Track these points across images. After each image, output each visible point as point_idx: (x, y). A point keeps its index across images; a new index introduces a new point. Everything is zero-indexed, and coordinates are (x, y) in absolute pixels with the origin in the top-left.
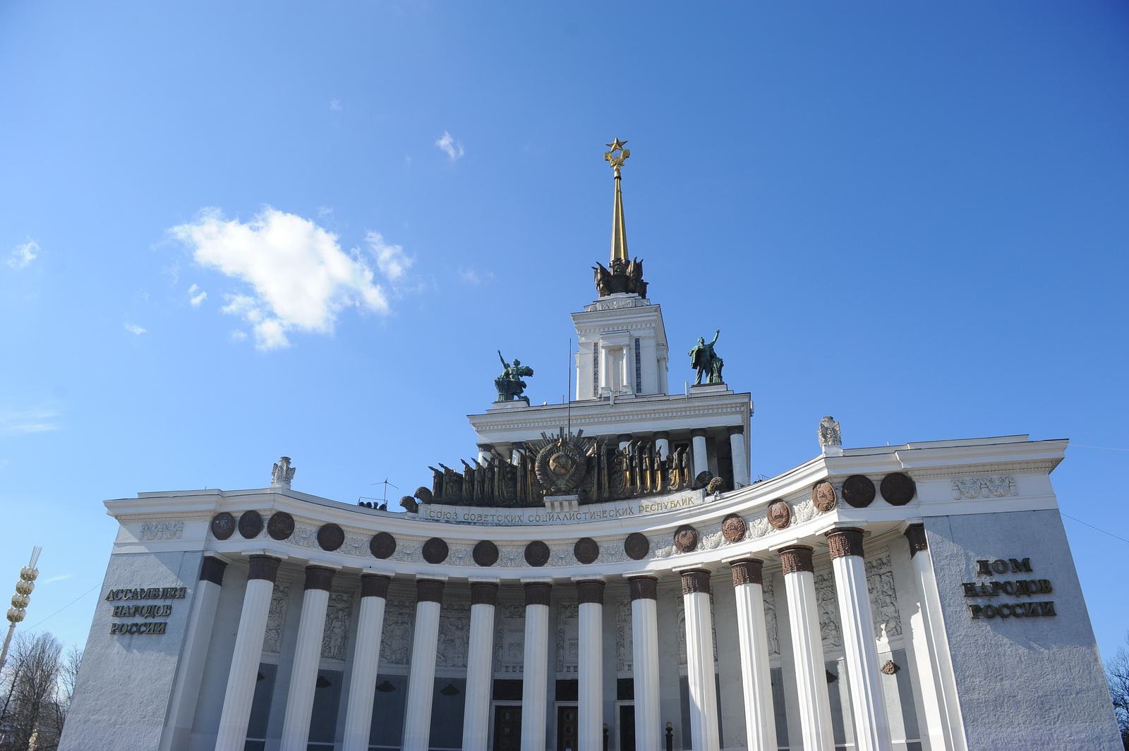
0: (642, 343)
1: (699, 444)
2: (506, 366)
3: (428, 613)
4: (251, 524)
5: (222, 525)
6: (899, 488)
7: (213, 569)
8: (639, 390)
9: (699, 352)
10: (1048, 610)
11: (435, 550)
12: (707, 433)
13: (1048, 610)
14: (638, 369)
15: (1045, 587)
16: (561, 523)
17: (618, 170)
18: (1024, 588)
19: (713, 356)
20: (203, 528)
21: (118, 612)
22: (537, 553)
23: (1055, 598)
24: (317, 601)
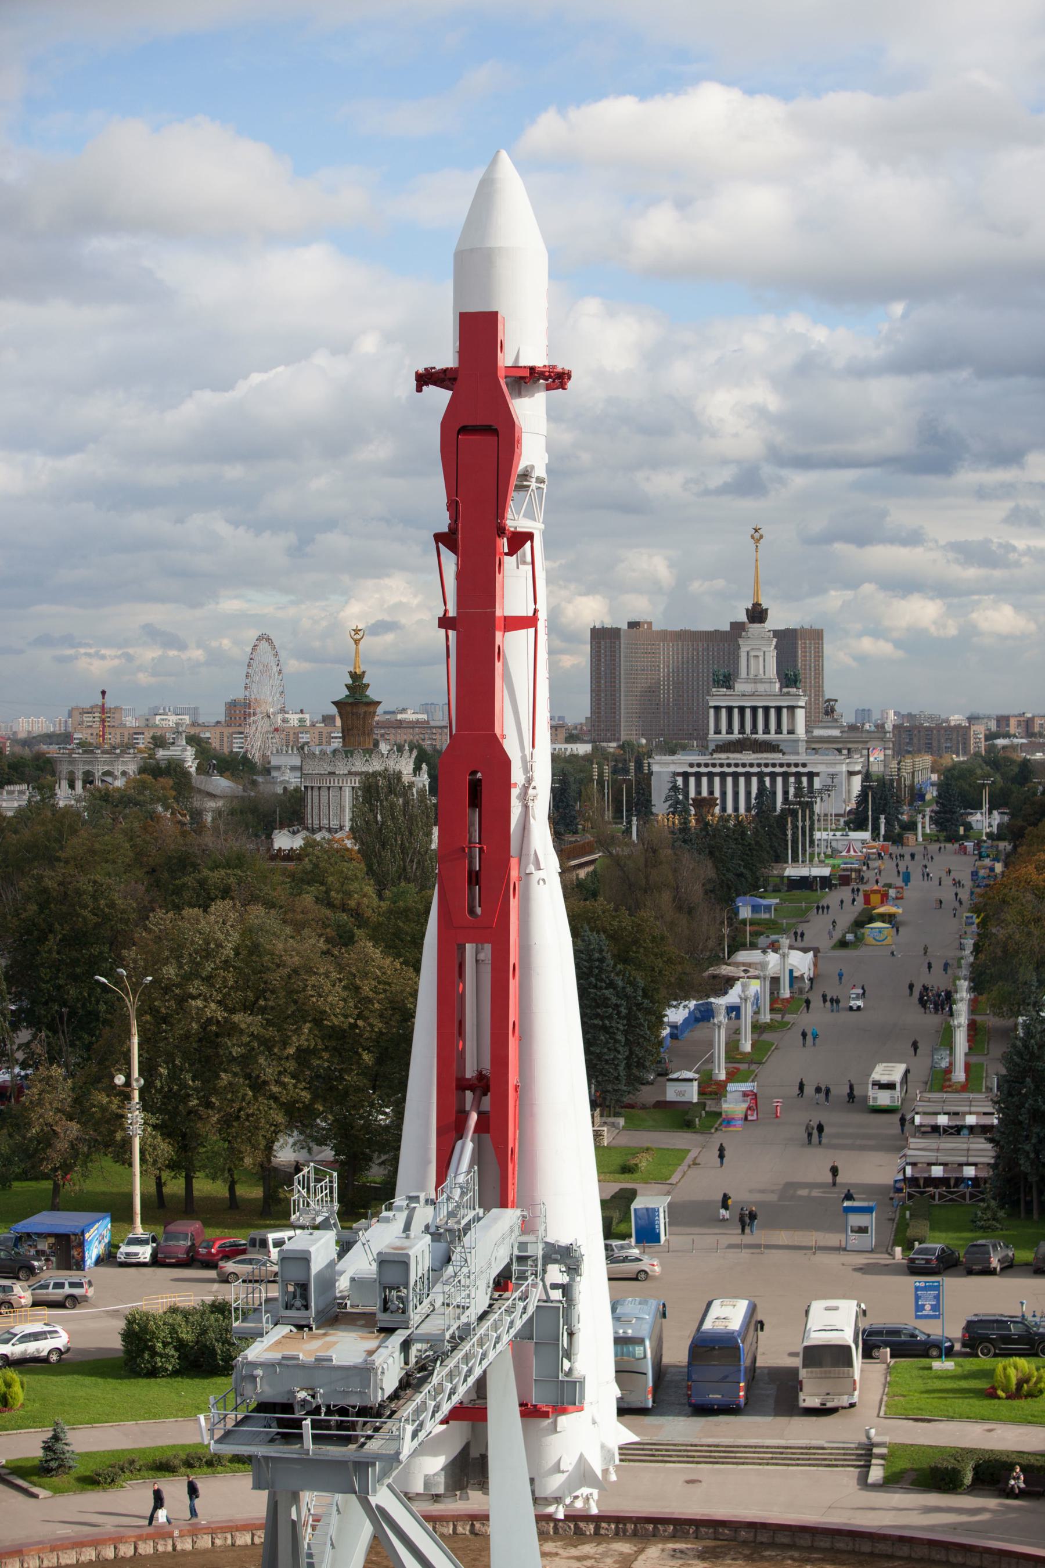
1: (785, 711)
12: (788, 707)
16: (748, 757)
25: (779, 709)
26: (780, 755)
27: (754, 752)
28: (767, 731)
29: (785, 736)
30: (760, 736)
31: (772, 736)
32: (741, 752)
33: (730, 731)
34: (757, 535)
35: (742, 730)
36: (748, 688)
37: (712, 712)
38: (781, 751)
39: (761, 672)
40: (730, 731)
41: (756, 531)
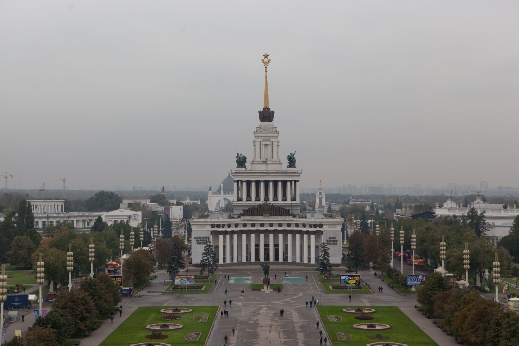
0: (274, 143)
2: (238, 154)
3: (244, 236)
4: (218, 226)
5: (213, 226)
6: (321, 226)
7: (212, 233)
8: (272, 158)
9: (290, 158)
10: (336, 244)
11: (245, 225)
12: (291, 181)
13: (336, 244)
14: (272, 151)
15: (337, 241)
16: (267, 219)
17: (266, 68)
18: (334, 241)
19: (294, 158)
20: (210, 227)
21: (197, 241)
22: (262, 225)
23: (338, 242)
24: (228, 236)
25: (284, 183)
26: (291, 218)
27: (271, 215)
28: (276, 198)
29: (289, 202)
30: (271, 202)
31: (280, 202)
32: (262, 215)
33: (249, 198)
34: (266, 60)
35: (258, 198)
36: (262, 168)
37: (235, 184)
38: (291, 215)
39: (270, 155)
40: (249, 198)
41: (266, 56)
